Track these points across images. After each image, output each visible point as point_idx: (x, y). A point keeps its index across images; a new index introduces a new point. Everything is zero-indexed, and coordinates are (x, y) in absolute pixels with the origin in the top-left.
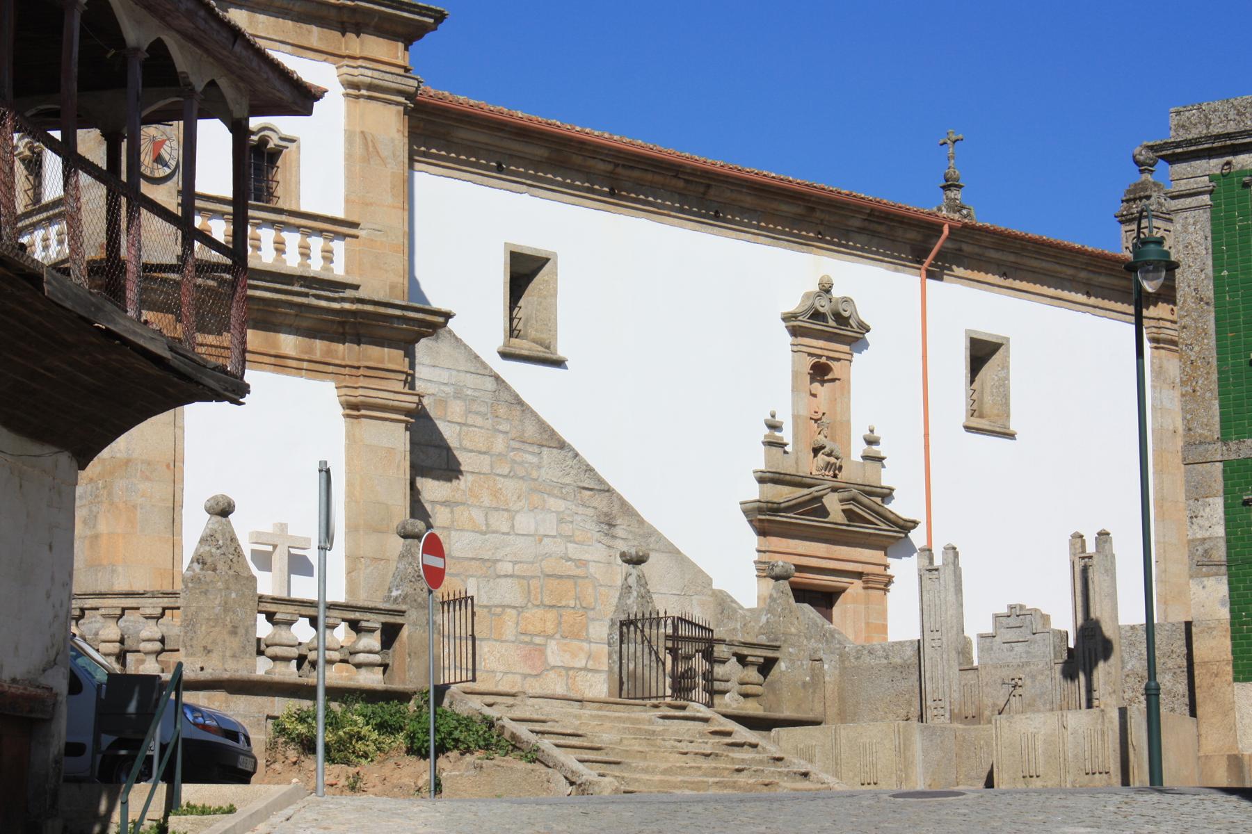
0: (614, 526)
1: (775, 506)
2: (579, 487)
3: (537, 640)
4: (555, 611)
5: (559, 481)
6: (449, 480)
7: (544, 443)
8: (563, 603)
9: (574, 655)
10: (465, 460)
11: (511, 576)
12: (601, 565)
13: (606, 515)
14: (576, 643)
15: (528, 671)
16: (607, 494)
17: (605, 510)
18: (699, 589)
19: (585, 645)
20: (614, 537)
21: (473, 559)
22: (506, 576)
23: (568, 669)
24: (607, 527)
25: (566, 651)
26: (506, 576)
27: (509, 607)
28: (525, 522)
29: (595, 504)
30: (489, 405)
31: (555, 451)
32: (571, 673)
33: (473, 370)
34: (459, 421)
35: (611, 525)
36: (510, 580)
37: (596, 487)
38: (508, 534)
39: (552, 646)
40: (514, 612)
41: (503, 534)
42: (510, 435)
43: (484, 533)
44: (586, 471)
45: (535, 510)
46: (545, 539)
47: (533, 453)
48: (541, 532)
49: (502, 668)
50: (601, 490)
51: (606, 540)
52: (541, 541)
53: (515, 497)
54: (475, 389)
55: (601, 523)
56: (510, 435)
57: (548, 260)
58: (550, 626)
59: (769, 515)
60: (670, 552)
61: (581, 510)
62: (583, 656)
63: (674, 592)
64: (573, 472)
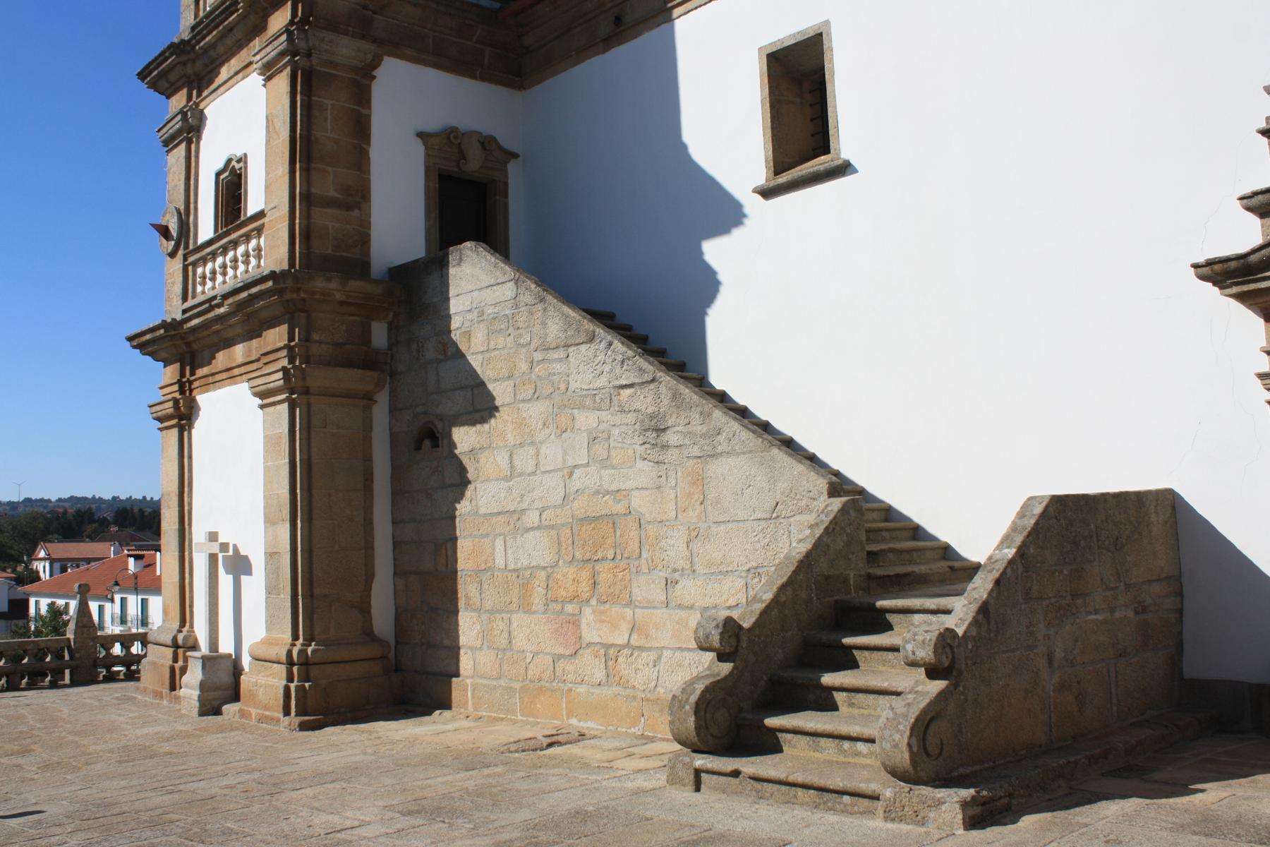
0: (665, 430)
1: (1233, 264)
2: (615, 387)
3: (570, 608)
4: (590, 566)
5: (591, 386)
6: (483, 421)
7: (569, 342)
8: (600, 555)
9: (615, 626)
10: (500, 392)
11: (539, 528)
12: (647, 492)
13: (652, 417)
14: (616, 609)
15: (560, 650)
16: (652, 386)
17: (650, 410)
18: (803, 503)
19: (628, 612)
20: (665, 447)
21: (499, 513)
22: (533, 529)
23: (607, 647)
24: (654, 435)
25: (603, 621)
26: (533, 529)
27: (538, 567)
28: (552, 453)
29: (638, 405)
30: (510, 317)
31: (583, 348)
32: (611, 651)
33: (492, 282)
34: (482, 349)
35: (661, 431)
36: (537, 533)
37: (637, 381)
38: (534, 473)
39: (588, 615)
40: (543, 574)
41: (529, 475)
42: (533, 346)
43: (508, 478)
44: (623, 362)
45: (564, 435)
46: (576, 471)
47: (560, 360)
48: (570, 463)
49: (534, 648)
50: (643, 383)
51: (654, 454)
52: (571, 474)
53: (540, 425)
54: (495, 305)
55: (645, 430)
56: (533, 346)
57: (821, 34)
58: (584, 587)
59: (1237, 284)
60: (751, 452)
61: (618, 419)
62: (625, 627)
63: (759, 516)
64: (607, 368)
